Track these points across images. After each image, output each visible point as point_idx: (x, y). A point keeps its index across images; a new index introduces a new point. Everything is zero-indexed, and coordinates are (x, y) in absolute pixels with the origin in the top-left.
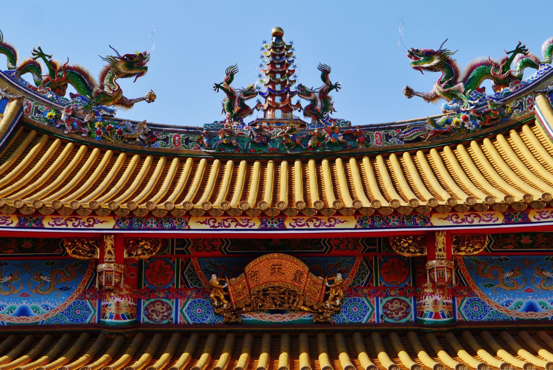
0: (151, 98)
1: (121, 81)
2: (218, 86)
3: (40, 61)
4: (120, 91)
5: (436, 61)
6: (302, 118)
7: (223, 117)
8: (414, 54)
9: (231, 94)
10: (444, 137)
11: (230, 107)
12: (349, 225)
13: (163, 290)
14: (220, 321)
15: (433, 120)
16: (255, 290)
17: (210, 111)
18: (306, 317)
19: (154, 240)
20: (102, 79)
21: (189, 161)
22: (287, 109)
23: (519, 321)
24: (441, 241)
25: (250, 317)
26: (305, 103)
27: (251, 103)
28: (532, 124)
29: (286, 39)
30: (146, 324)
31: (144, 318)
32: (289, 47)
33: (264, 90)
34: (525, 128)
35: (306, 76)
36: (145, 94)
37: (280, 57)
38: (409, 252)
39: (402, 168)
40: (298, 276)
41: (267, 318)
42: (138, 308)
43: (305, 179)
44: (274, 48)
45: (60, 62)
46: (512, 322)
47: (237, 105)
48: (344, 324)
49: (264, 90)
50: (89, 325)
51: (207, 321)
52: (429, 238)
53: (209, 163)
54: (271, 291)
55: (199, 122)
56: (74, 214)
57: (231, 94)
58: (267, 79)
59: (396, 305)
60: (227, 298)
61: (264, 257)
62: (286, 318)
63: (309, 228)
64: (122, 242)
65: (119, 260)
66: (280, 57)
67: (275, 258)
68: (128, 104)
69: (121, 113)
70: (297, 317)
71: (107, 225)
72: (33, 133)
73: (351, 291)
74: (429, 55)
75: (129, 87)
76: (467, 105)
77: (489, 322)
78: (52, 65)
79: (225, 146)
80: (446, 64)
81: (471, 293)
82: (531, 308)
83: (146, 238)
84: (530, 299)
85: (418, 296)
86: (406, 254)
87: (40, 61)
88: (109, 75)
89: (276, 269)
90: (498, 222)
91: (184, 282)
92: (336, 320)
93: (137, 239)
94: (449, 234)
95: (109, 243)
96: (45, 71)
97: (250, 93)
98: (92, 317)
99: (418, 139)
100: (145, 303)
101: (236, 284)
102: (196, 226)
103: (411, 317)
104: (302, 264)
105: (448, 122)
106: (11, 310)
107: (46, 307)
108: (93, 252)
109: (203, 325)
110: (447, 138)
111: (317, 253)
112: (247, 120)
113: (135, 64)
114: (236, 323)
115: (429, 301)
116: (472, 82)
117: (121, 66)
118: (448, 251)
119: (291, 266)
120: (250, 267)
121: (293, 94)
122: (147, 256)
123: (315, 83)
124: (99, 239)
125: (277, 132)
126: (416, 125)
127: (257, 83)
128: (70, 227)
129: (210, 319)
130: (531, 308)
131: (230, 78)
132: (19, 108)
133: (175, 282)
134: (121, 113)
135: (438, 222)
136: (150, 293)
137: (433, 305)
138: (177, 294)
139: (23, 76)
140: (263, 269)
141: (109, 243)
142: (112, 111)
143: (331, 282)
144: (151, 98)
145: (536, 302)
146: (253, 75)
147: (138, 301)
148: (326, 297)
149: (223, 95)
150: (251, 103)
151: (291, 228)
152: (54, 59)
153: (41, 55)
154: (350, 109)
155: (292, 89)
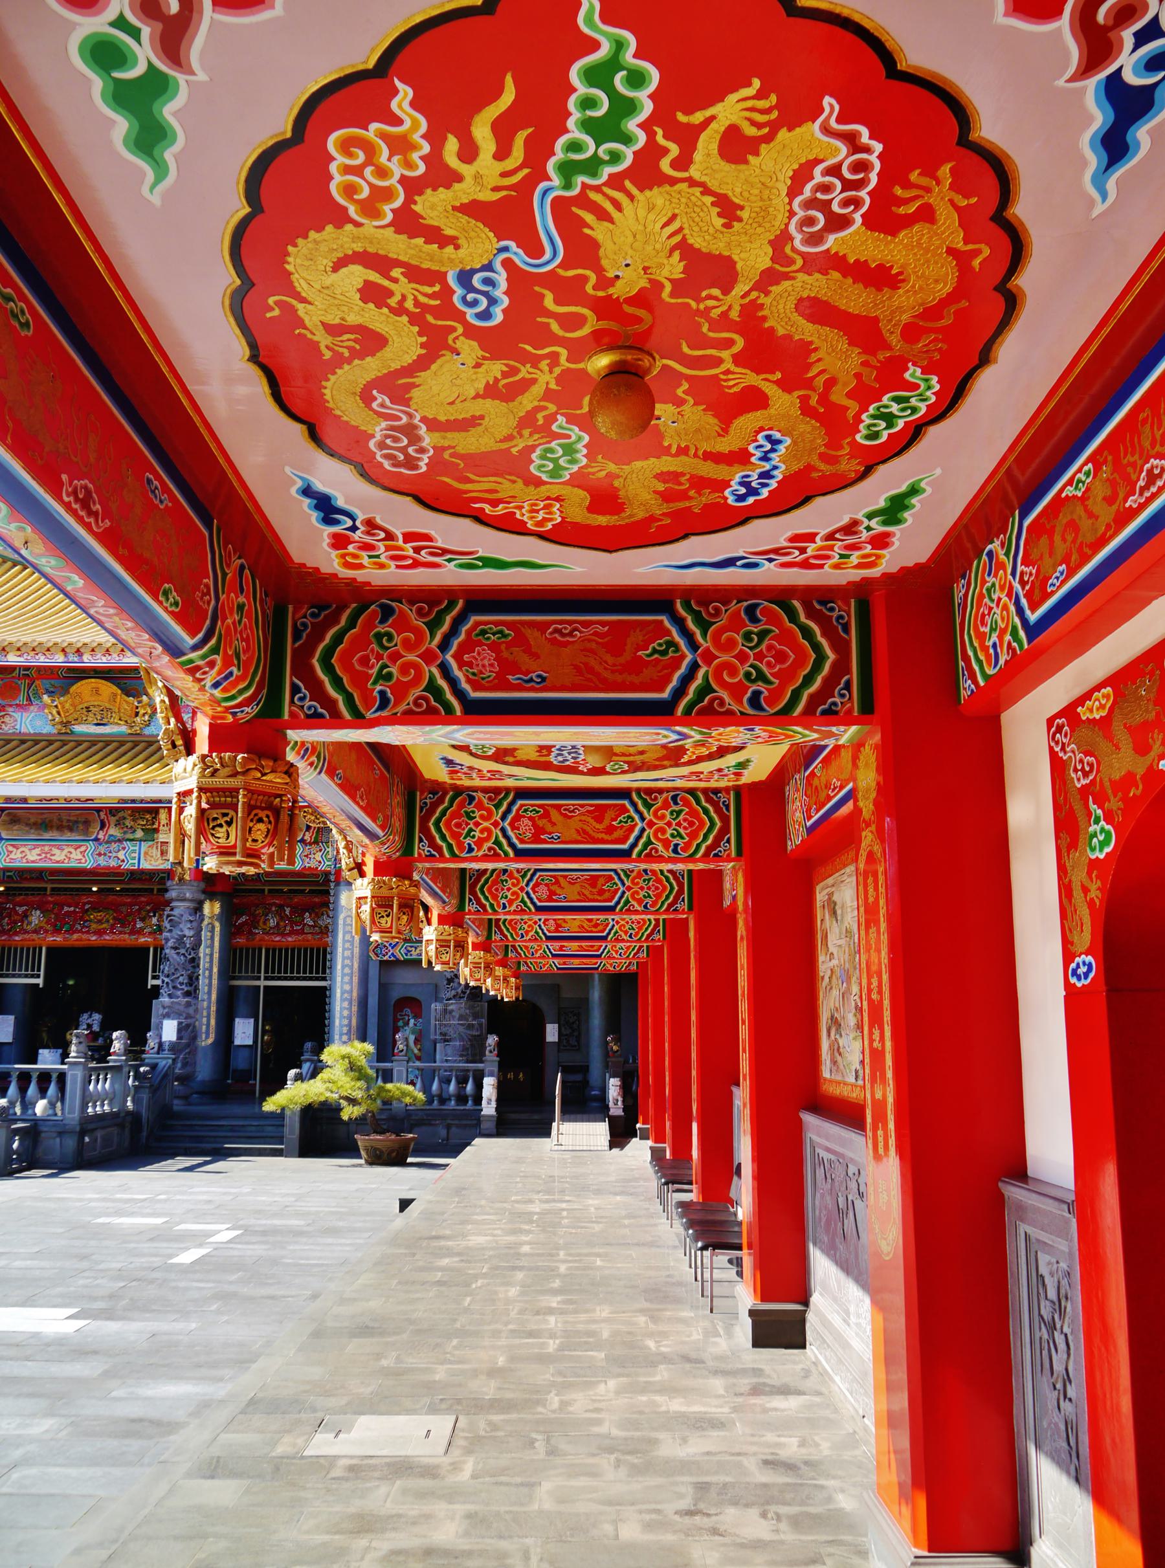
13: (11, 706)
14: (55, 731)
18: (123, 729)
25: (79, 728)
51: (44, 732)
54: (92, 708)
60: (59, 713)
61: (84, 682)
67: (93, 682)
89: (97, 691)
91: (29, 699)
101: (65, 701)
104: (115, 688)
114: (66, 733)
119: (108, 689)
120: (73, 689)
129: (48, 729)
133: (22, 699)
143: (140, 702)
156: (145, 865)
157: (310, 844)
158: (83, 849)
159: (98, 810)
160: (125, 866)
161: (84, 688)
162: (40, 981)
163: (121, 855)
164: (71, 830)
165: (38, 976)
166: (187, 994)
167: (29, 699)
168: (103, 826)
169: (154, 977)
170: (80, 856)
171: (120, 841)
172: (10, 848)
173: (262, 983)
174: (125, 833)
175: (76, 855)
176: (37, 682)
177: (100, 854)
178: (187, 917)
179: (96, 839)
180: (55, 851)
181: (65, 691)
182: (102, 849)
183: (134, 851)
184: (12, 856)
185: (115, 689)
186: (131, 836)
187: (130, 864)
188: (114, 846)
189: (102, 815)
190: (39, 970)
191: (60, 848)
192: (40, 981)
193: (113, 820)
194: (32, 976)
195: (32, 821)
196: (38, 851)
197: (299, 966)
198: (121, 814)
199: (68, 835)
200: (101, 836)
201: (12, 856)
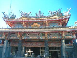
8: (49, 11)
17: (35, 16)
24: (47, 21)
35: (42, 13)
37: (40, 12)
55: (35, 16)
56: (21, 20)
66: (40, 12)
69: (29, 16)
71: (23, 21)
73: (41, 26)
74: (50, 11)
75: (30, 14)
79: (36, 18)
80: (51, 12)
82: (54, 26)
89: (36, 24)
101: (33, 25)
111: (38, 22)
116: (53, 13)
119: (36, 24)
120: (34, 24)
123: (42, 13)
128: (21, 21)
134: (29, 16)
137: (47, 26)
140: (35, 24)
154: (45, 15)
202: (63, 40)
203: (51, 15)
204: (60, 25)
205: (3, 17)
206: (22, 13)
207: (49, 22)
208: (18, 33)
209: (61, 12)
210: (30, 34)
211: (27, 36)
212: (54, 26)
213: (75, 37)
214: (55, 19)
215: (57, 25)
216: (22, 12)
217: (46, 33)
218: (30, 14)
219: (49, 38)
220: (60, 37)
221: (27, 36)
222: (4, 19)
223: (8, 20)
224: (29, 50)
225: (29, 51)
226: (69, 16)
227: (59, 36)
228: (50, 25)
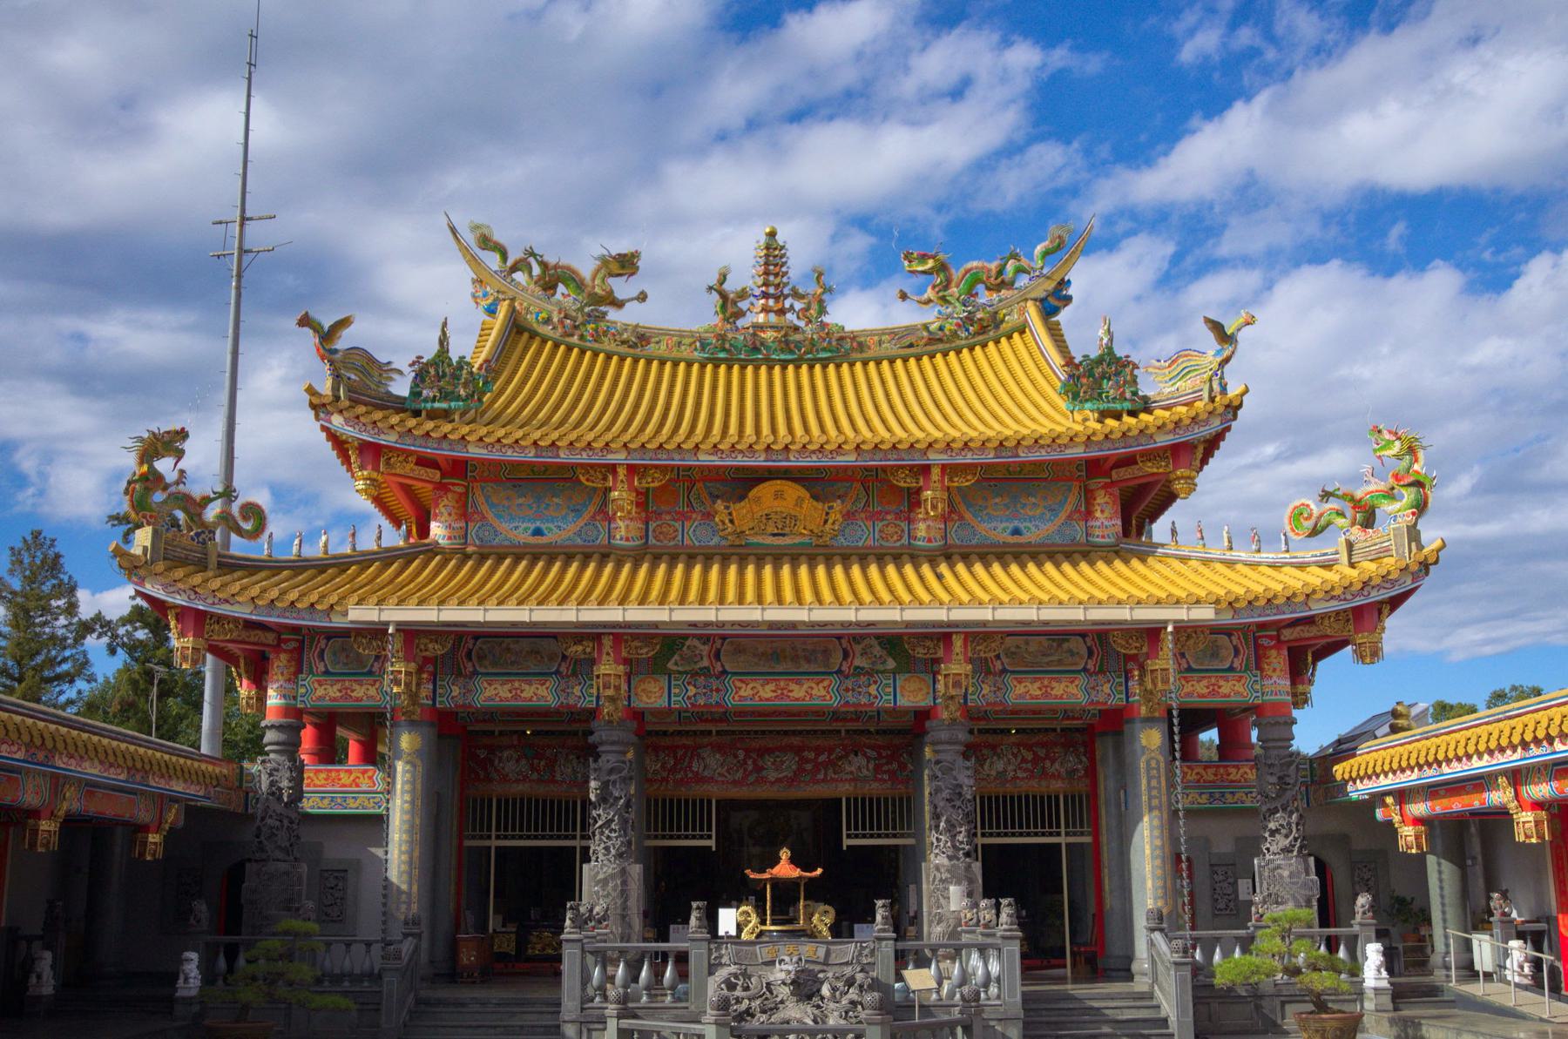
0: (642, 297)
1: (611, 281)
2: (711, 288)
3: (532, 260)
4: (611, 292)
5: (931, 263)
6: (796, 322)
7: (716, 320)
9: (724, 296)
10: (934, 343)
11: (724, 307)
12: (849, 459)
14: (724, 543)
15: (926, 327)
16: (757, 516)
17: (703, 317)
18: (806, 540)
19: (664, 469)
20: (593, 279)
21: (682, 366)
22: (781, 312)
23: (1005, 545)
24: (935, 473)
26: (798, 305)
27: (743, 305)
28: (1022, 332)
29: (780, 238)
30: (654, 546)
31: (652, 541)
32: (782, 248)
33: (757, 292)
34: (1016, 336)
36: (635, 294)
38: (905, 482)
39: (895, 377)
40: (799, 502)
41: (770, 540)
42: (647, 530)
43: (799, 388)
44: (767, 248)
45: (551, 260)
46: (999, 546)
47: (730, 305)
48: (842, 547)
49: (757, 292)
50: (600, 546)
51: (712, 543)
52: (926, 470)
53: (703, 367)
57: (724, 296)
58: (760, 281)
59: (890, 530)
60: (732, 521)
62: (787, 541)
63: (813, 461)
64: (632, 469)
65: (631, 488)
67: (778, 484)
68: (619, 304)
69: (613, 315)
70: (797, 540)
71: (619, 457)
72: (526, 336)
75: (622, 288)
76: (960, 312)
77: (976, 546)
78: (544, 265)
81: (961, 518)
83: (656, 467)
84: (1016, 523)
85: (910, 521)
86: (902, 484)
87: (532, 260)
88: (600, 275)
90: (989, 457)
91: (690, 504)
92: (834, 543)
93: (645, 467)
94: (944, 467)
95: (622, 472)
96: (536, 270)
97: (743, 294)
98: (602, 539)
99: (911, 346)
100: (652, 525)
101: (741, 510)
102: (705, 459)
103: (905, 541)
105: (941, 329)
106: (526, 530)
107: (559, 527)
108: (605, 479)
109: (709, 547)
110: (941, 346)
111: (819, 481)
112: (740, 323)
113: (626, 264)
115: (922, 526)
117: (615, 268)
118: (942, 481)
119: (793, 491)
120: (753, 493)
121: (786, 297)
122: (656, 484)
124: (613, 468)
125: (769, 335)
126: (911, 330)
127: (750, 283)
128: (584, 458)
130: (1016, 532)
131: (723, 278)
132: (513, 311)
135: (935, 458)
136: (659, 515)
138: (683, 517)
139: (514, 276)
141: (622, 472)
142: (605, 314)
144: (642, 297)
145: (1022, 526)
146: (746, 274)
147: (647, 523)
148: (826, 522)
149: (715, 296)
150: (743, 305)
151: (794, 461)
152: (546, 258)
153: (532, 254)
155: (786, 291)
156: (903, 702)
157: (1096, 673)
158: (826, 683)
159: (839, 637)
160: (879, 704)
161: (765, 491)
162: (712, 843)
163: (873, 690)
164: (809, 661)
165: (709, 837)
166: (967, 855)
167: (690, 504)
168: (846, 655)
169: (849, 836)
170: (823, 692)
171: (869, 673)
172: (739, 684)
173: (980, 841)
174: (873, 663)
175: (819, 691)
176: (698, 485)
177: (847, 690)
178: (960, 761)
179: (839, 672)
180: (793, 686)
181: (742, 498)
182: (849, 683)
183: (887, 685)
184: (742, 693)
185: (802, 492)
186: (881, 667)
187: (886, 701)
188: (863, 679)
189: (844, 641)
190: (710, 829)
191: (798, 683)
192: (712, 843)
193: (858, 648)
194: (702, 837)
195: (761, 650)
196: (771, 687)
197: (894, 820)
198: (867, 642)
199: (805, 667)
200: (845, 668)
201: (742, 693)
202: (1150, 720)
203: (930, 316)
204: (1089, 514)
205: (325, 387)
206: (492, 261)
207: (959, 482)
208: (607, 642)
209: (1120, 352)
210: (739, 651)
211: (695, 674)
212: (1016, 532)
213: (1286, 683)
214: (1041, 455)
215: (1063, 515)
216: (486, 242)
217: (958, 643)
218: (622, 288)
219: (984, 694)
220: (1108, 694)
221: (695, 674)
222: (337, 421)
223: (389, 439)
224: (785, 854)
225: (785, 869)
226: (1216, 425)
227: (1102, 672)
228: (962, 508)
